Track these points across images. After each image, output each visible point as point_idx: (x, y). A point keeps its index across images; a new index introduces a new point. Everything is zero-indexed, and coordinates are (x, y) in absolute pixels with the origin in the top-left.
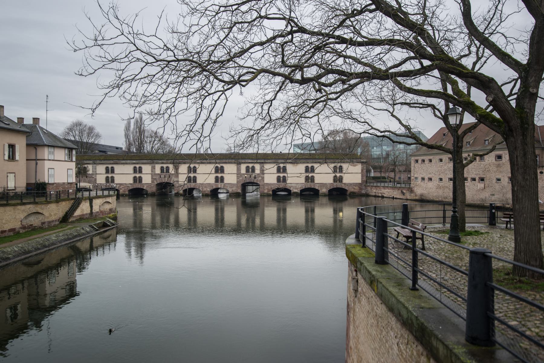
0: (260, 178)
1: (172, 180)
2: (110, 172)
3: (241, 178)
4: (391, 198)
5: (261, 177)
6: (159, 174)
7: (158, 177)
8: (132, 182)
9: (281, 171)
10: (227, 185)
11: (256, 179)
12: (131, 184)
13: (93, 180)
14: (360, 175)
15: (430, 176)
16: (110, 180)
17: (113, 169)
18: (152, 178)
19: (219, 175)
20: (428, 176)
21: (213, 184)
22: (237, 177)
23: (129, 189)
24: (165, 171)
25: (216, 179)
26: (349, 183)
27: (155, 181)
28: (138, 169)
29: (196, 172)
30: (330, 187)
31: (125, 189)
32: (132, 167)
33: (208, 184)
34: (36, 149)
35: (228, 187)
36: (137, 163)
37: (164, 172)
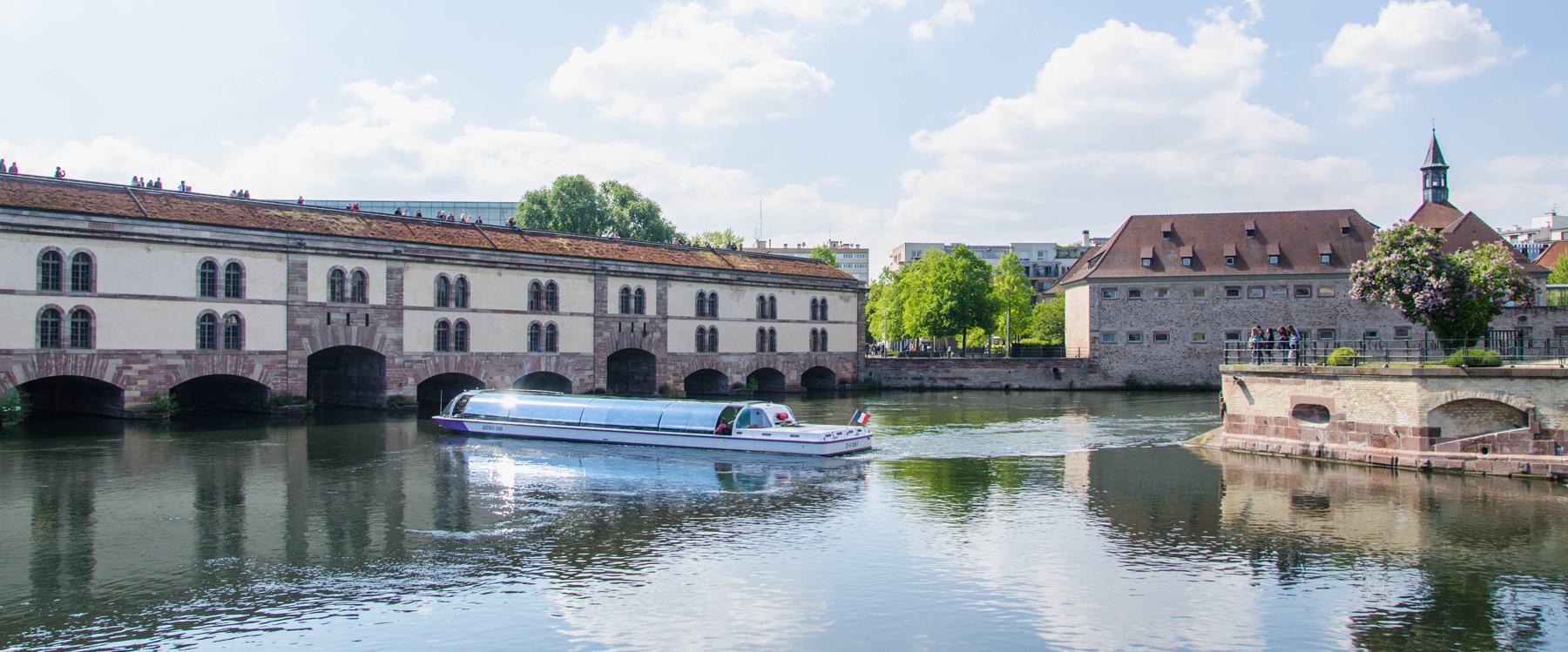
0: (657, 335)
1: (378, 337)
2: (67, 282)
3: (607, 334)
4: (1000, 389)
5: (661, 330)
6: (322, 305)
7: (317, 321)
8: (189, 340)
9: (707, 309)
10: (566, 360)
12: (185, 355)
14: (855, 327)
15: (1161, 329)
16: (66, 329)
17: (84, 265)
19: (544, 320)
20: (1153, 329)
21: (524, 355)
22: (595, 327)
23: (175, 381)
24: (348, 295)
26: (838, 354)
27: (305, 341)
31: (152, 385)
32: (192, 259)
35: (570, 368)
37: (343, 300)
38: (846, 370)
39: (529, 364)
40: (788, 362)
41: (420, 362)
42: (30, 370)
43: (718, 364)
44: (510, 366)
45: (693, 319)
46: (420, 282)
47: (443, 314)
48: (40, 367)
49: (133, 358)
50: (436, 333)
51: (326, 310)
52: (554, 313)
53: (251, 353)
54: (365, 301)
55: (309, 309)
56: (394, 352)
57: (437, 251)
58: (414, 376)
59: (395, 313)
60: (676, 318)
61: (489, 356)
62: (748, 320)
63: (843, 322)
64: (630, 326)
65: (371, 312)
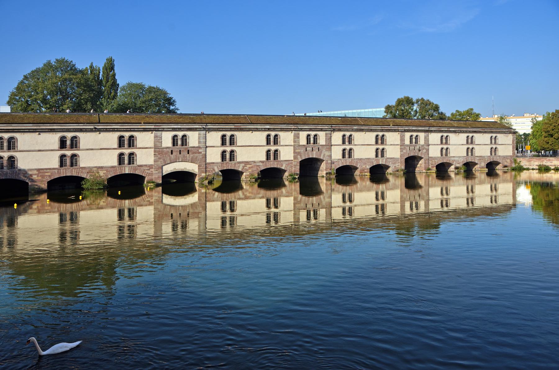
0: (425, 151)
5: (426, 149)
6: (304, 146)
7: (302, 150)
8: (264, 158)
9: (444, 141)
12: (262, 162)
13: (200, 156)
18: (294, 152)
21: (373, 159)
22: (401, 149)
26: (503, 156)
27: (299, 156)
30: (488, 160)
31: (253, 171)
33: (367, 159)
35: (391, 163)
36: (274, 130)
38: (507, 162)
39: (375, 162)
40: (480, 159)
41: (337, 162)
42: (219, 168)
43: (450, 160)
45: (439, 145)
47: (344, 147)
48: (222, 167)
49: (247, 163)
53: (282, 161)
59: (328, 147)
60: (432, 145)
61: (361, 159)
62: (462, 145)
63: (505, 144)
65: (319, 147)
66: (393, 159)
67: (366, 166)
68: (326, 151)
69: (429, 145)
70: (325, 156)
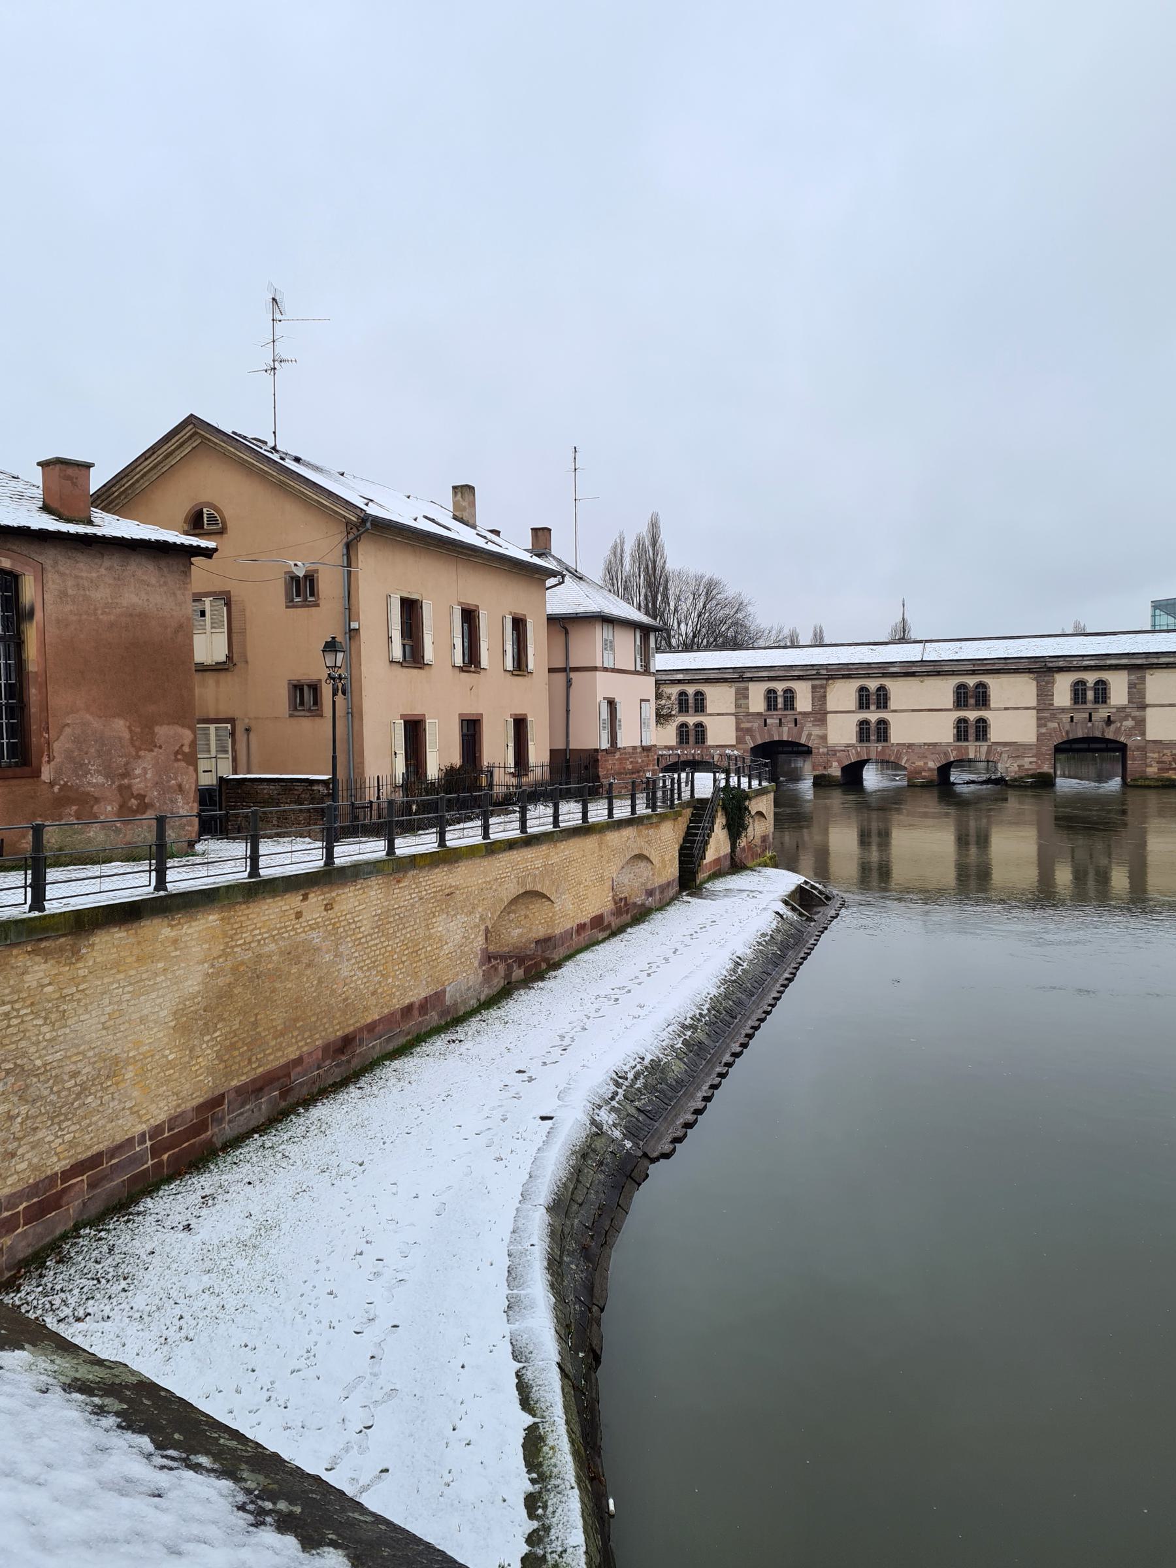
0: (1129, 723)
3: (1053, 725)
5: (1134, 718)
6: (759, 714)
7: (756, 725)
11: (1113, 727)
18: (738, 729)
19: (972, 715)
21: (949, 745)
22: (1038, 719)
25: (958, 728)
27: (748, 738)
28: (691, 701)
29: (885, 707)
34: (567, 633)
35: (1005, 756)
37: (776, 709)
39: (955, 752)
41: (844, 751)
44: (932, 754)
46: (843, 695)
50: (858, 729)
51: (763, 717)
52: (983, 708)
53: (711, 747)
54: (793, 708)
55: (750, 717)
56: (819, 744)
57: (857, 668)
58: (838, 761)
59: (819, 716)
61: (910, 746)
64: (1087, 715)
65: (797, 717)
66: (1012, 748)
67: (926, 763)
68: (813, 725)
69: (1146, 706)
70: (812, 737)
